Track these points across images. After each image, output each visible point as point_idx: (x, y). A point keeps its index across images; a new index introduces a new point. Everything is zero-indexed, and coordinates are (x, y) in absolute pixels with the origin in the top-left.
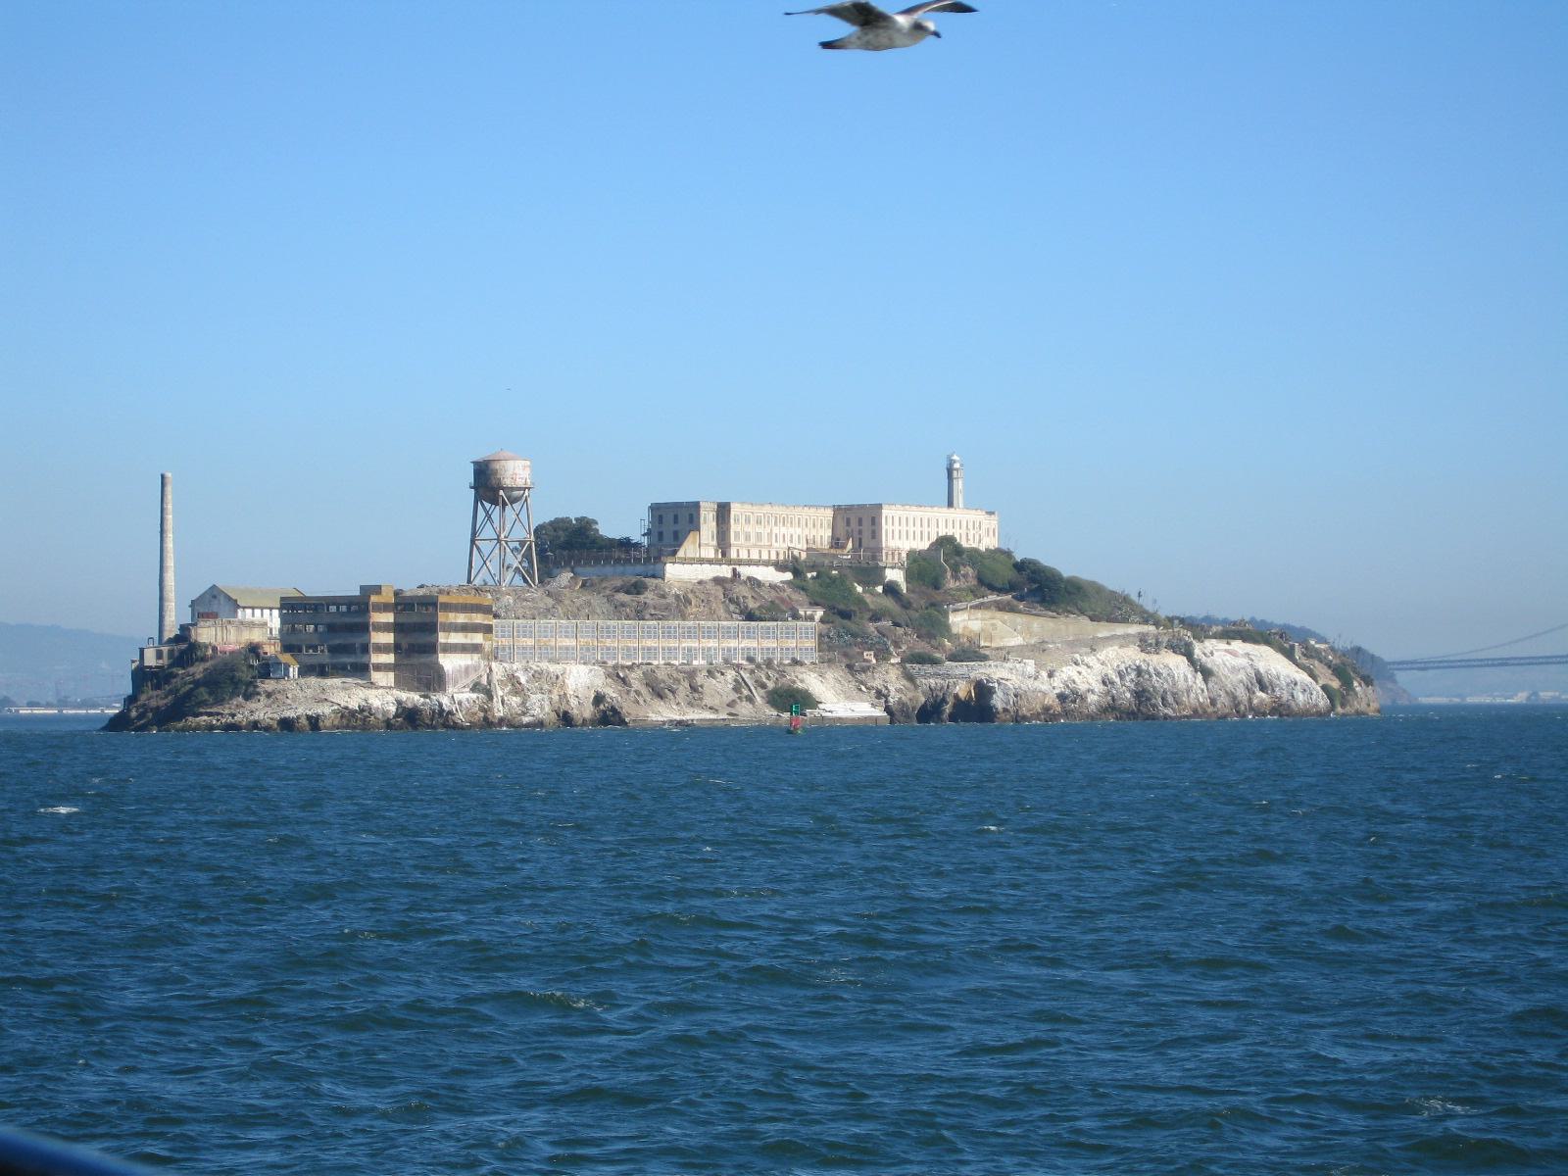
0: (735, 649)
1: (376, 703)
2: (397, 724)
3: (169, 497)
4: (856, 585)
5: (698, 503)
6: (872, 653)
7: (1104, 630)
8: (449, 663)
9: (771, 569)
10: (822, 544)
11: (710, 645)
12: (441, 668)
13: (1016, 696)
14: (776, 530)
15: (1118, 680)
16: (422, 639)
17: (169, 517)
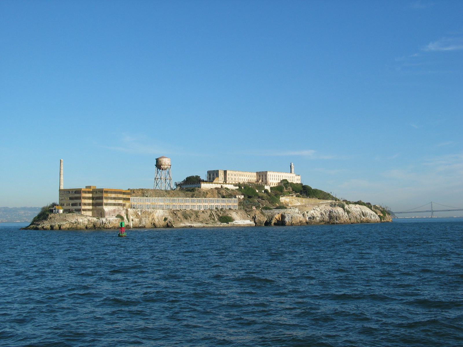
0: (213, 206)
1: (81, 221)
2: (90, 227)
3: (62, 166)
4: (256, 190)
5: (218, 170)
6: (255, 207)
7: (321, 201)
8: (106, 209)
9: (232, 186)
10: (253, 181)
11: (206, 205)
12: (104, 210)
13: (291, 218)
14: (240, 177)
15: (325, 214)
16: (99, 201)
17: (62, 171)
